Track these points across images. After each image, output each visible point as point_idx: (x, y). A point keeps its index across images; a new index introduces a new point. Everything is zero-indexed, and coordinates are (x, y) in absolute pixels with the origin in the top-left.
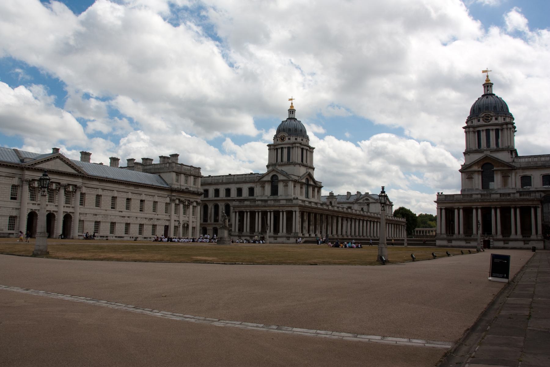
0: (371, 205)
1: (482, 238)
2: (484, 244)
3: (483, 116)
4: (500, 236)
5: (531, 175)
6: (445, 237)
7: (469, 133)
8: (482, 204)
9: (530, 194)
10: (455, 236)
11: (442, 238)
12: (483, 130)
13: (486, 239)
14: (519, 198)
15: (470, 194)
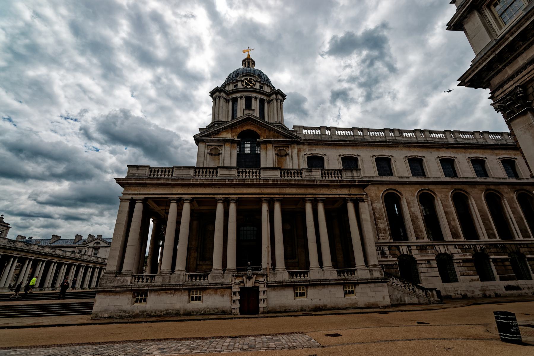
0: (101, 249)
1: (238, 280)
2: (240, 301)
3: (243, 80)
4: (284, 276)
5: (324, 155)
6: (129, 283)
7: (219, 99)
8: (238, 191)
9: (341, 174)
10: (158, 280)
11: (116, 287)
12: (241, 97)
13: (249, 284)
14: (321, 179)
15: (213, 168)
